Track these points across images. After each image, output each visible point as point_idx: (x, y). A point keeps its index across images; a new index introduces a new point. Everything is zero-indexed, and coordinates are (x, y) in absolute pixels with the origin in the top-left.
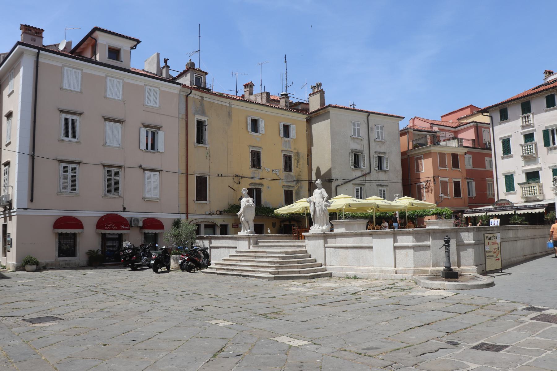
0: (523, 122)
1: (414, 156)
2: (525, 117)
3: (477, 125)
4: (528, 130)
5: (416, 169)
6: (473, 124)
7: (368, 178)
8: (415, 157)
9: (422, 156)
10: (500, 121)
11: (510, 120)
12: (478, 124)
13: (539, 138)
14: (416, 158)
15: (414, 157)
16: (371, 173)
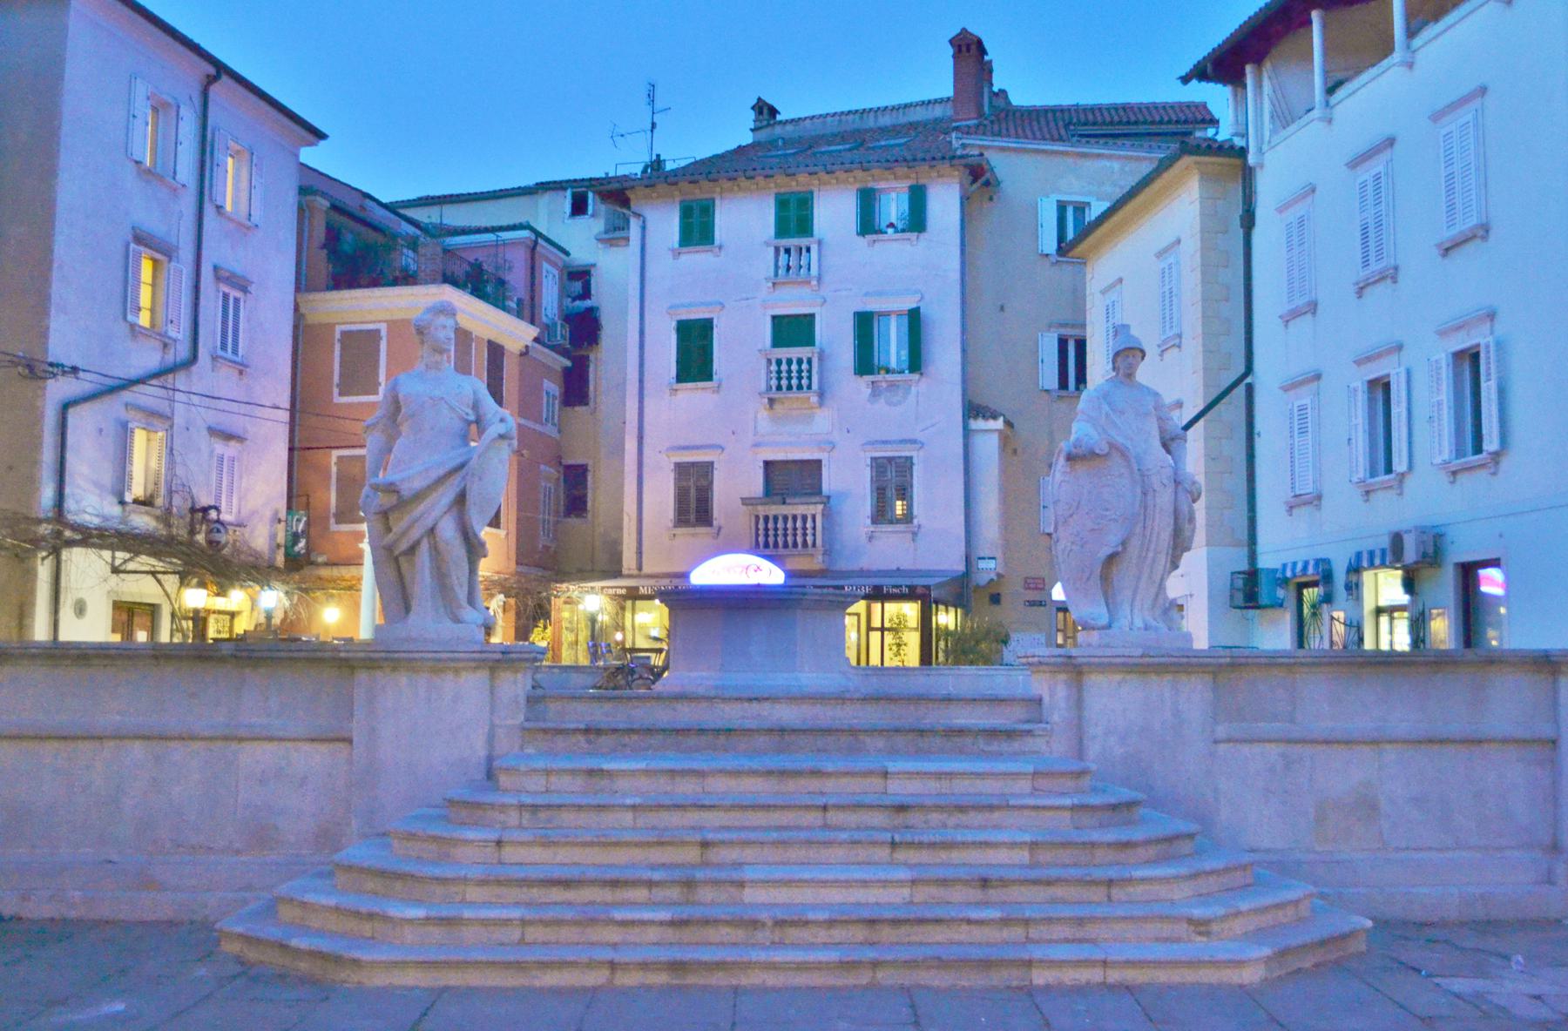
0: (777, 267)
1: (335, 324)
2: (788, 251)
3: (536, 243)
4: (792, 302)
5: (336, 379)
6: (525, 233)
7: (180, 380)
8: (338, 329)
9: (383, 327)
10: (676, 245)
11: (720, 247)
12: (540, 240)
13: (834, 333)
14: (344, 333)
15: (335, 324)
16: (194, 368)
